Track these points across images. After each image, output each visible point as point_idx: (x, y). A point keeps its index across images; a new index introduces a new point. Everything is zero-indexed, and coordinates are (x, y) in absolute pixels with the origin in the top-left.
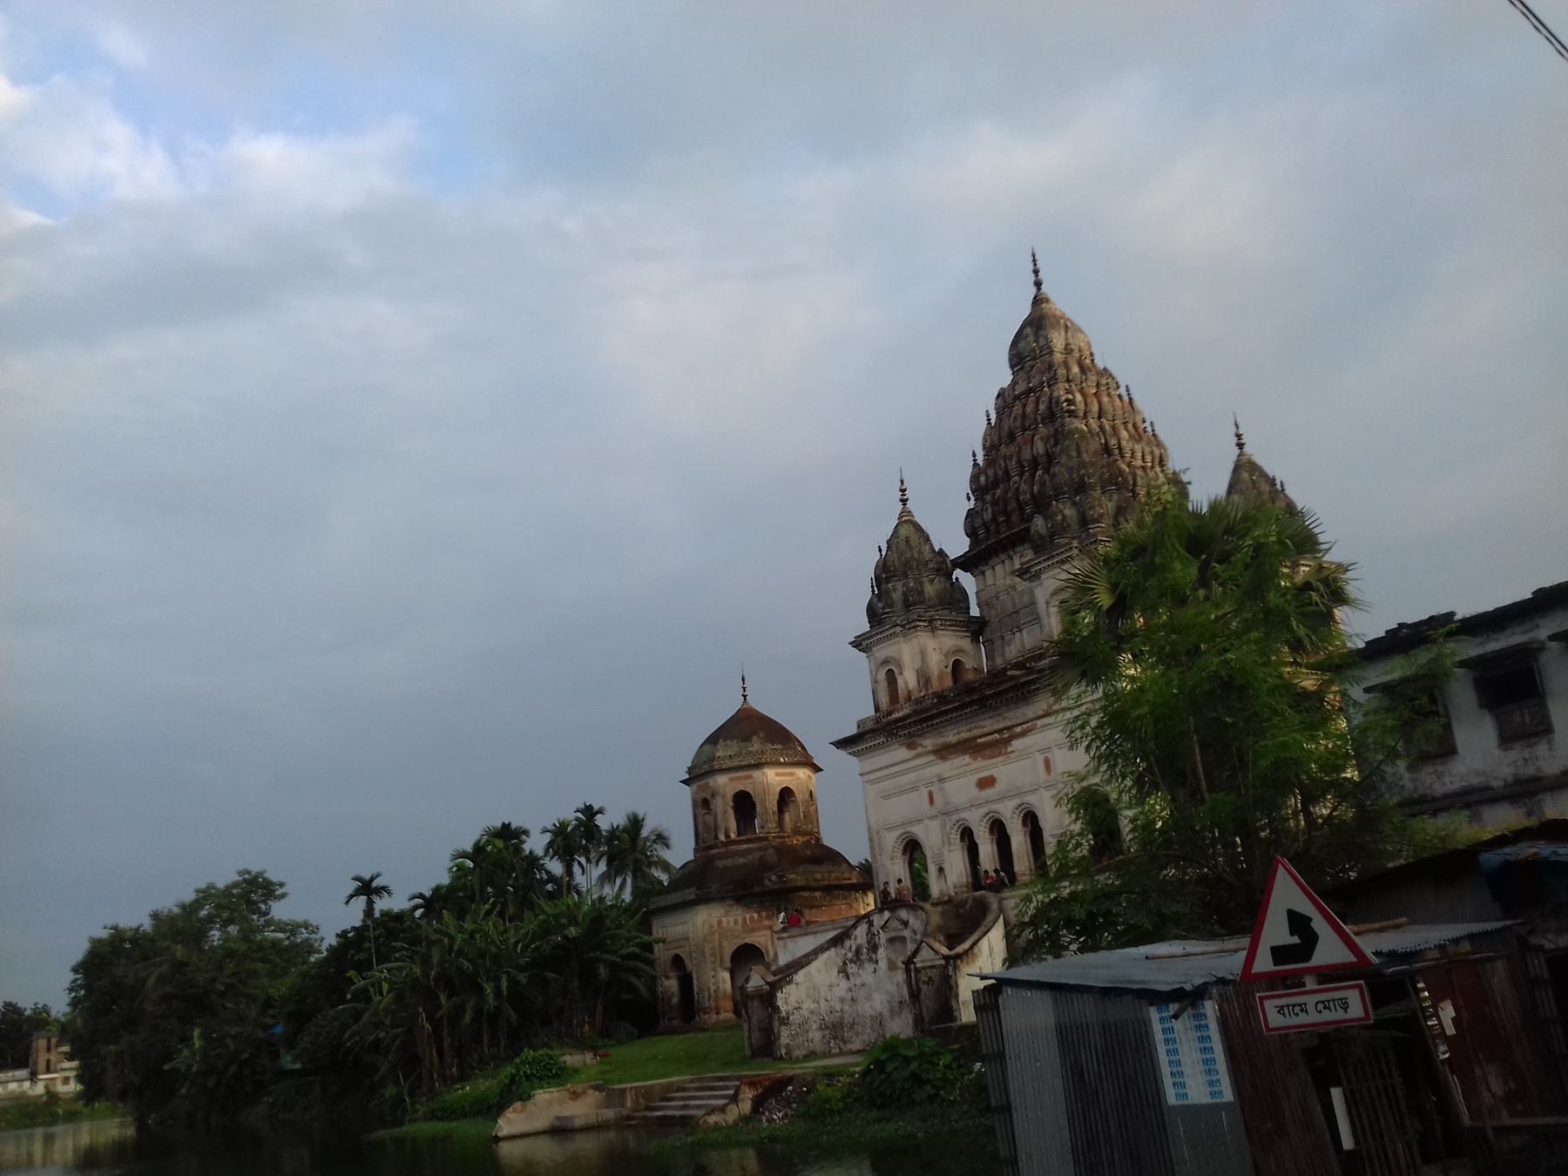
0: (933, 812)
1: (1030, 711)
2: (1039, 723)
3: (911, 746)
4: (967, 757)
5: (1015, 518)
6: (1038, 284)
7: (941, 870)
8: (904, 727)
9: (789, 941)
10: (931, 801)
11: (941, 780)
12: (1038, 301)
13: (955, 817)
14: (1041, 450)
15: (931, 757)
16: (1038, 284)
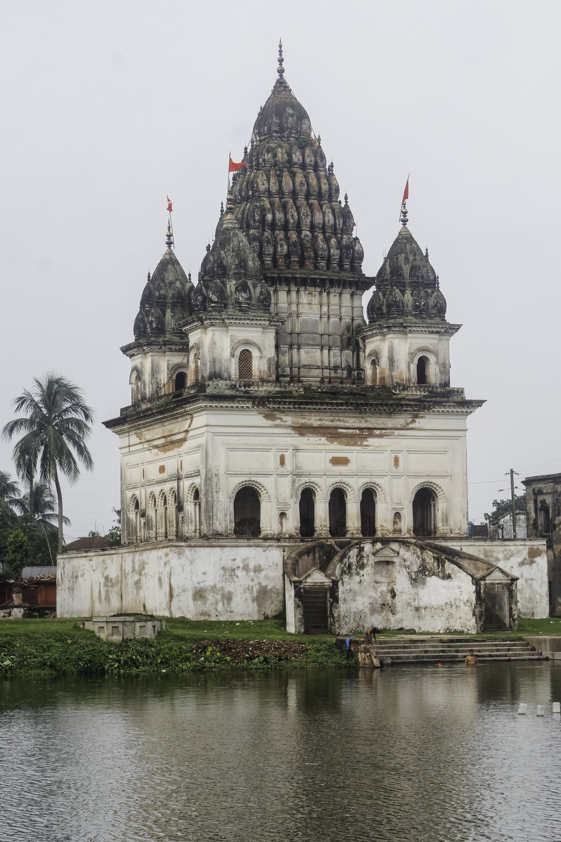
0: (281, 470)
1: (389, 422)
2: (397, 432)
3: (267, 417)
4: (324, 439)
5: (309, 264)
6: (281, 71)
7: (283, 515)
8: (279, 403)
9: (187, 551)
10: (282, 462)
11: (296, 450)
12: (281, 86)
13: (304, 480)
14: (332, 222)
15: (289, 431)
16: (281, 71)
